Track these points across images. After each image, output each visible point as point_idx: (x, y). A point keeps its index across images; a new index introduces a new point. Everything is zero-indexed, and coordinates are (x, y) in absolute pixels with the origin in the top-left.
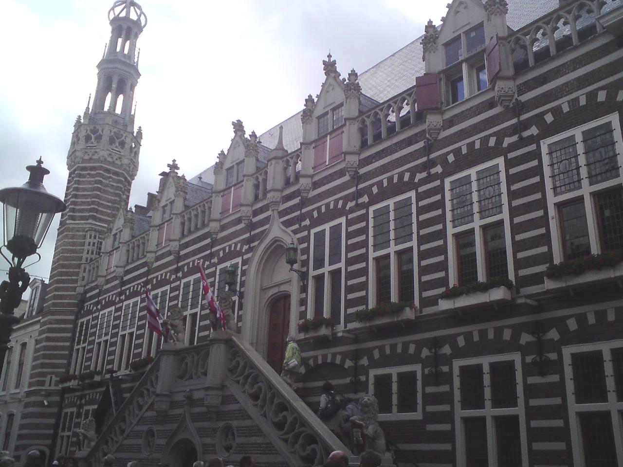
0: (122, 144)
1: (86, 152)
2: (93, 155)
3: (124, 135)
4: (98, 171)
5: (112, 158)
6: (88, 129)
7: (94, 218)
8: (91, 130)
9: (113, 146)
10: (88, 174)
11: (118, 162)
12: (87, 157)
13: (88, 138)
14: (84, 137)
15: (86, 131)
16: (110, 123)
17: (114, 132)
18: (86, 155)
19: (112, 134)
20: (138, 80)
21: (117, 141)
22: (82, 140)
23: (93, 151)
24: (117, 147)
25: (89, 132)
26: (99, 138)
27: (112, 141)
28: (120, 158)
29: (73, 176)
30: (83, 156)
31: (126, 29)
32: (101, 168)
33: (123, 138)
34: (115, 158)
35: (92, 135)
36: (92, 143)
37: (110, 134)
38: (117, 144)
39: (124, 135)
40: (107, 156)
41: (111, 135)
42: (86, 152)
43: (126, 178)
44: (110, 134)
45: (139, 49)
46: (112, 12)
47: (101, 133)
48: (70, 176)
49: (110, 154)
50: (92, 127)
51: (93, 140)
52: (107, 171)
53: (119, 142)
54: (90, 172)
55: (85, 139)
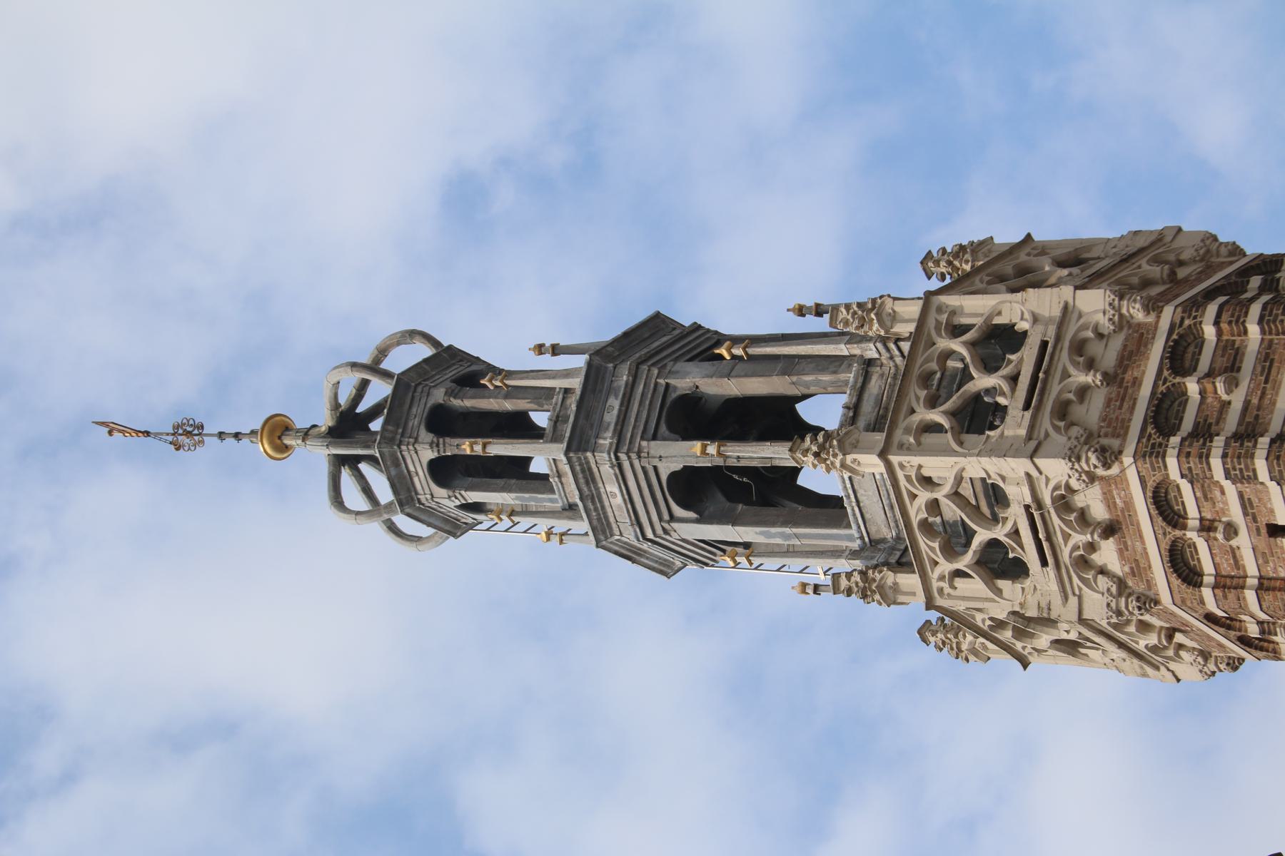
0: (998, 341)
1: (1083, 563)
2: (1083, 518)
6: (946, 567)
8: (951, 551)
9: (1013, 402)
11: (1109, 355)
12: (1108, 554)
13: (1000, 565)
14: (1003, 584)
15: (959, 582)
16: (880, 437)
17: (932, 403)
21: (982, 382)
24: (1014, 379)
25: (964, 562)
30: (1103, 582)
34: (1081, 378)
35: (977, 542)
36: (1015, 533)
40: (1075, 431)
42: (1083, 563)
43: (1210, 295)
49: (1062, 411)
50: (928, 547)
51: (1000, 533)
53: (990, 366)
54: (1193, 523)
55: (1003, 575)
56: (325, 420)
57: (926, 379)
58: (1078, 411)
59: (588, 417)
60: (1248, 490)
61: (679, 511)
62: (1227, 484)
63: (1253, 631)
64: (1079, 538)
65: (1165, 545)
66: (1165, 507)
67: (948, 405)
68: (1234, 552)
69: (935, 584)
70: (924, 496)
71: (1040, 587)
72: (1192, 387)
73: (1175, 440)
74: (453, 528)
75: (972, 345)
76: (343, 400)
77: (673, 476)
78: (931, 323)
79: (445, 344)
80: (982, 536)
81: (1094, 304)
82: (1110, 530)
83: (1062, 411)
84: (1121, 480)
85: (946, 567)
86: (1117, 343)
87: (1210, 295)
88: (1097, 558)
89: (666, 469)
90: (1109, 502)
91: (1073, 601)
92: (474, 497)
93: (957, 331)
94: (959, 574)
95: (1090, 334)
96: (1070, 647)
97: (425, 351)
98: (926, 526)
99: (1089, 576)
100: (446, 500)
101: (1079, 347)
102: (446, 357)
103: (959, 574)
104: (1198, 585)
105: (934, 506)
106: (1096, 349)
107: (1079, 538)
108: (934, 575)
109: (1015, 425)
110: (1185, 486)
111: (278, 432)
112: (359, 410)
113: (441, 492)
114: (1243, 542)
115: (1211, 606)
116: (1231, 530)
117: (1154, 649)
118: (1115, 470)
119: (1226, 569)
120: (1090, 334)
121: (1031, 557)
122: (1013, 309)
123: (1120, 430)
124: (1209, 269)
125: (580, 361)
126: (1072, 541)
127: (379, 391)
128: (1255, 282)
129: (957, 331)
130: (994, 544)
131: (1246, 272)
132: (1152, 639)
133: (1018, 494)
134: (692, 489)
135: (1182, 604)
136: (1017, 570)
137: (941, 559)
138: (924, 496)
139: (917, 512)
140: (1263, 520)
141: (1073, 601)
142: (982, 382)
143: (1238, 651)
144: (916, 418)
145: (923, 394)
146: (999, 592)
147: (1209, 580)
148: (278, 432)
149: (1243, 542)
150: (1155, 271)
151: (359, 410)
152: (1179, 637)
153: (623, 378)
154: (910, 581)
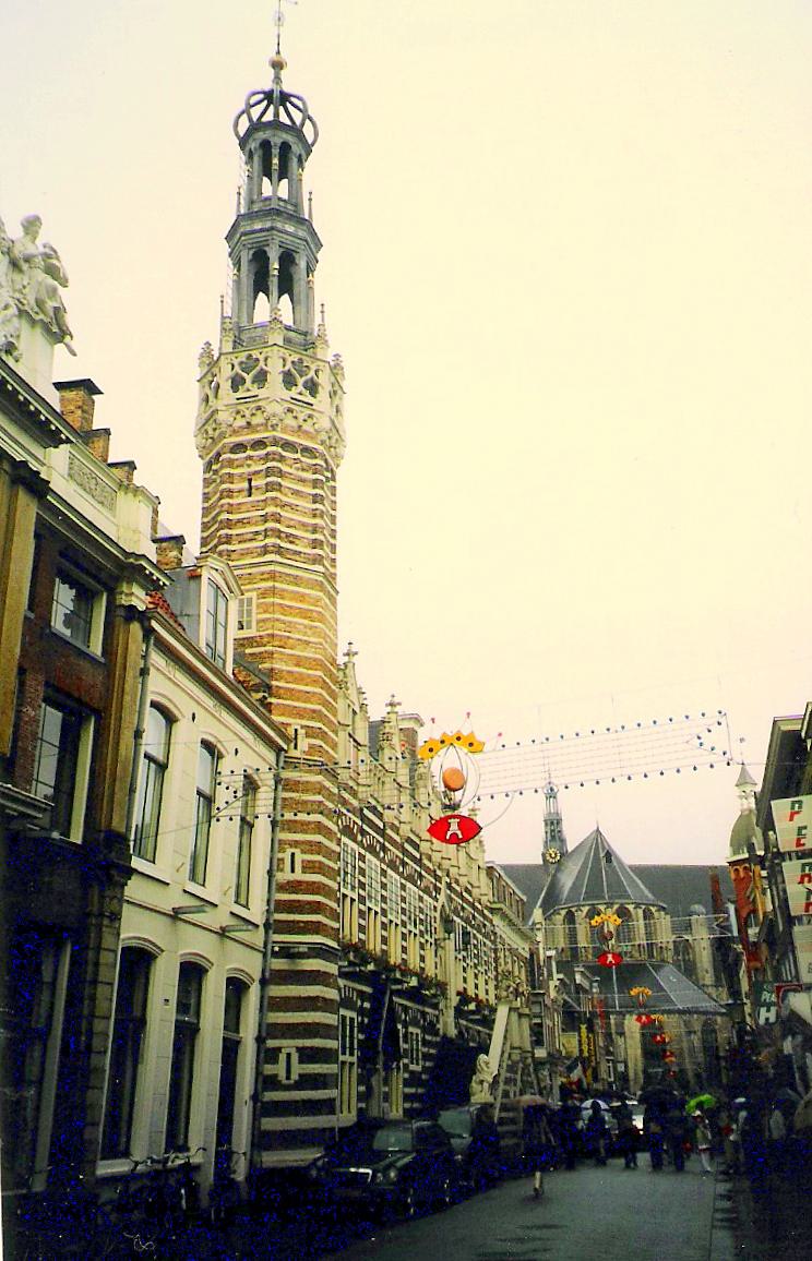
0: (312, 387)
1: (238, 412)
2: (253, 415)
3: (313, 367)
4: (269, 449)
5: (296, 417)
6: (236, 362)
7: (279, 550)
9: (294, 393)
10: (250, 458)
11: (306, 427)
12: (241, 422)
13: (237, 383)
15: (230, 366)
17: (293, 362)
18: (238, 417)
19: (289, 366)
20: (319, 256)
21: (301, 381)
22: (226, 386)
23: (254, 405)
24: (300, 394)
25: (237, 368)
26: (261, 378)
27: (289, 381)
28: (310, 416)
29: (214, 467)
31: (275, 145)
32: (275, 442)
33: (312, 374)
34: (301, 417)
35: (244, 375)
36: (248, 390)
37: (284, 366)
38: (300, 387)
39: (313, 367)
41: (286, 368)
43: (326, 461)
44: (284, 366)
45: (311, 193)
46: (245, 115)
47: (264, 367)
48: (208, 467)
49: (290, 410)
50: (243, 357)
52: (287, 445)
56: (287, 89)
57: (301, 361)
58: (290, 415)
59: (287, 219)
60: (264, 473)
61: (251, 252)
62: (265, 466)
63: (214, 467)
64: (247, 413)
65: (245, 443)
66: (260, 444)
67: (293, 370)
68: (242, 466)
69: (229, 356)
70: (261, 357)
71: (227, 395)
72: (298, 456)
73: (280, 450)
74: (243, 142)
75: (312, 379)
76: (293, 99)
77: (265, 252)
78: (321, 364)
79: (313, 149)
80: (248, 378)
81: (325, 423)
82: (248, 423)
83: (290, 410)
84: (267, 430)
85: (236, 362)
86: (312, 430)
87: (326, 461)
88: (238, 417)
89: (266, 249)
90: (258, 425)
91: (224, 408)
92: (256, 158)
93: (317, 372)
94: (233, 366)
95: (315, 420)
96: (207, 399)
97: (310, 142)
98: (251, 355)
99: (234, 414)
100: (253, 145)
101: (310, 416)
102: (308, 149)
103: (233, 366)
104: (231, 452)
105: (257, 360)
107: (247, 413)
108: (233, 356)
109: (287, 395)
110: (264, 452)
111: (278, 66)
112: (288, 104)
113: (258, 142)
114: (245, 470)
115: (224, 456)
116: (249, 466)
117: (207, 432)
118: (270, 428)
119: (236, 463)
120: (315, 420)
121: (239, 395)
122: (323, 393)
123: (284, 430)
124: (332, 458)
125: (307, 217)
126: (246, 410)
127: (297, 116)
128: (330, 475)
129: (317, 372)
131: (332, 471)
132: (211, 432)
133: (262, 393)
134: (260, 258)
135: (224, 446)
136: (235, 388)
137: (239, 360)
138: (261, 357)
139: (255, 354)
140: (253, 477)
141: (224, 408)
143: (208, 458)
144: (287, 356)
145: (296, 360)
146: (227, 380)
147: (233, 456)
148: (278, 66)
149: (245, 470)
150: (333, 441)
151: (288, 104)
152: (210, 441)
153: (301, 234)
154: (228, 347)
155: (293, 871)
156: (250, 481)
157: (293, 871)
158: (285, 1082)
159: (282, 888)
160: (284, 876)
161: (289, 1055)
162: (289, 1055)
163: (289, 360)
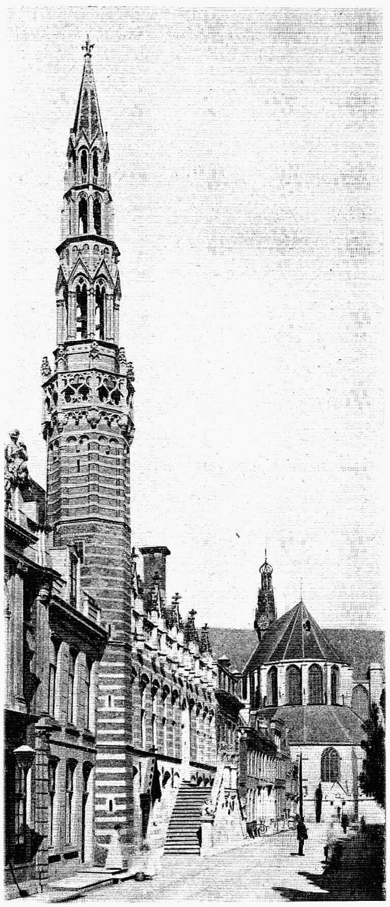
1: (70, 414)
13: (68, 392)
22: (61, 397)
27: (103, 393)
38: (109, 398)
101: (116, 416)
106: (115, 420)
130: (73, 393)
136: (68, 399)
142: (110, 393)
155: (110, 705)
156: (78, 462)
157: (110, 705)
158: (109, 813)
159: (104, 715)
160: (106, 709)
161: (111, 801)
162: (111, 801)
163: (103, 377)
